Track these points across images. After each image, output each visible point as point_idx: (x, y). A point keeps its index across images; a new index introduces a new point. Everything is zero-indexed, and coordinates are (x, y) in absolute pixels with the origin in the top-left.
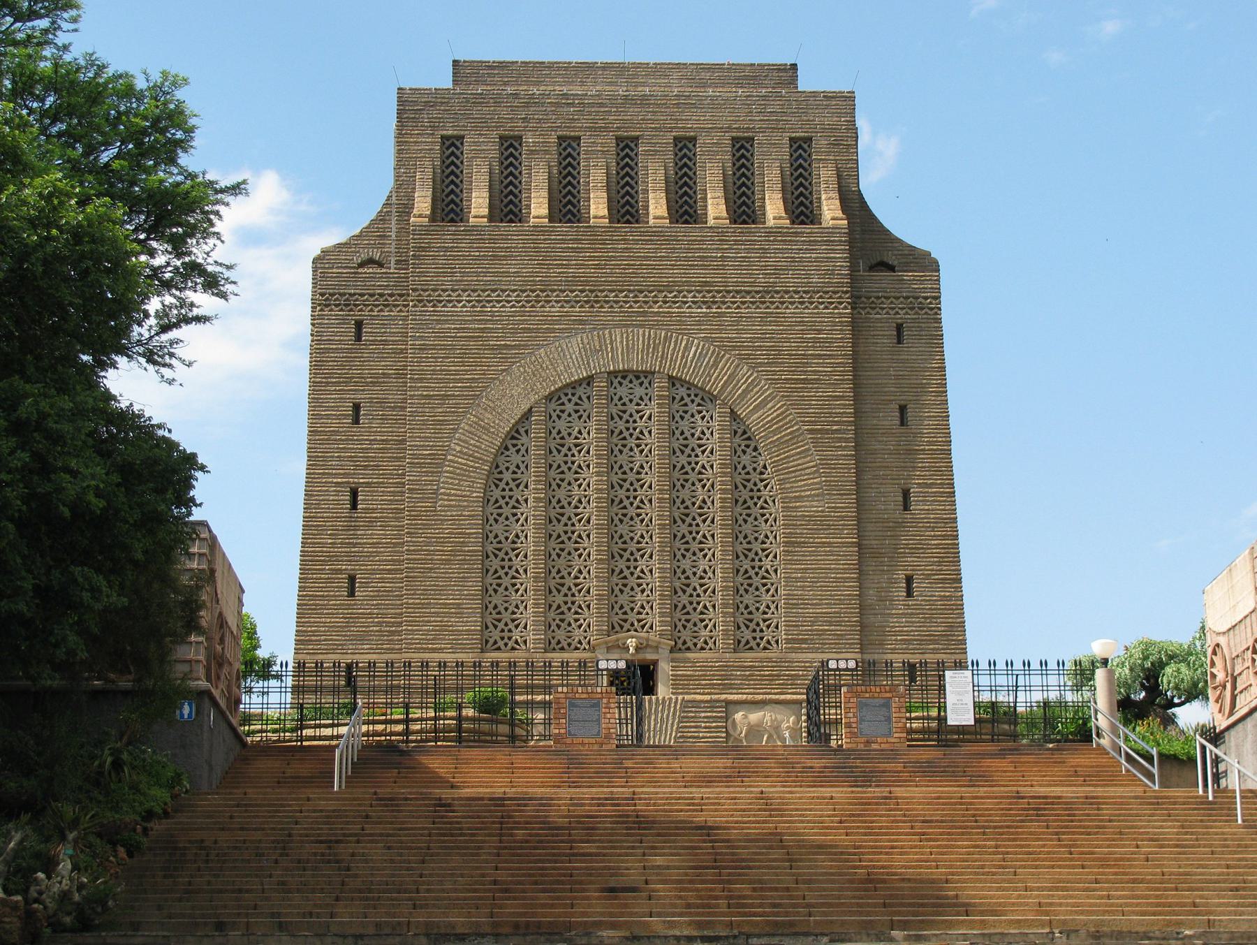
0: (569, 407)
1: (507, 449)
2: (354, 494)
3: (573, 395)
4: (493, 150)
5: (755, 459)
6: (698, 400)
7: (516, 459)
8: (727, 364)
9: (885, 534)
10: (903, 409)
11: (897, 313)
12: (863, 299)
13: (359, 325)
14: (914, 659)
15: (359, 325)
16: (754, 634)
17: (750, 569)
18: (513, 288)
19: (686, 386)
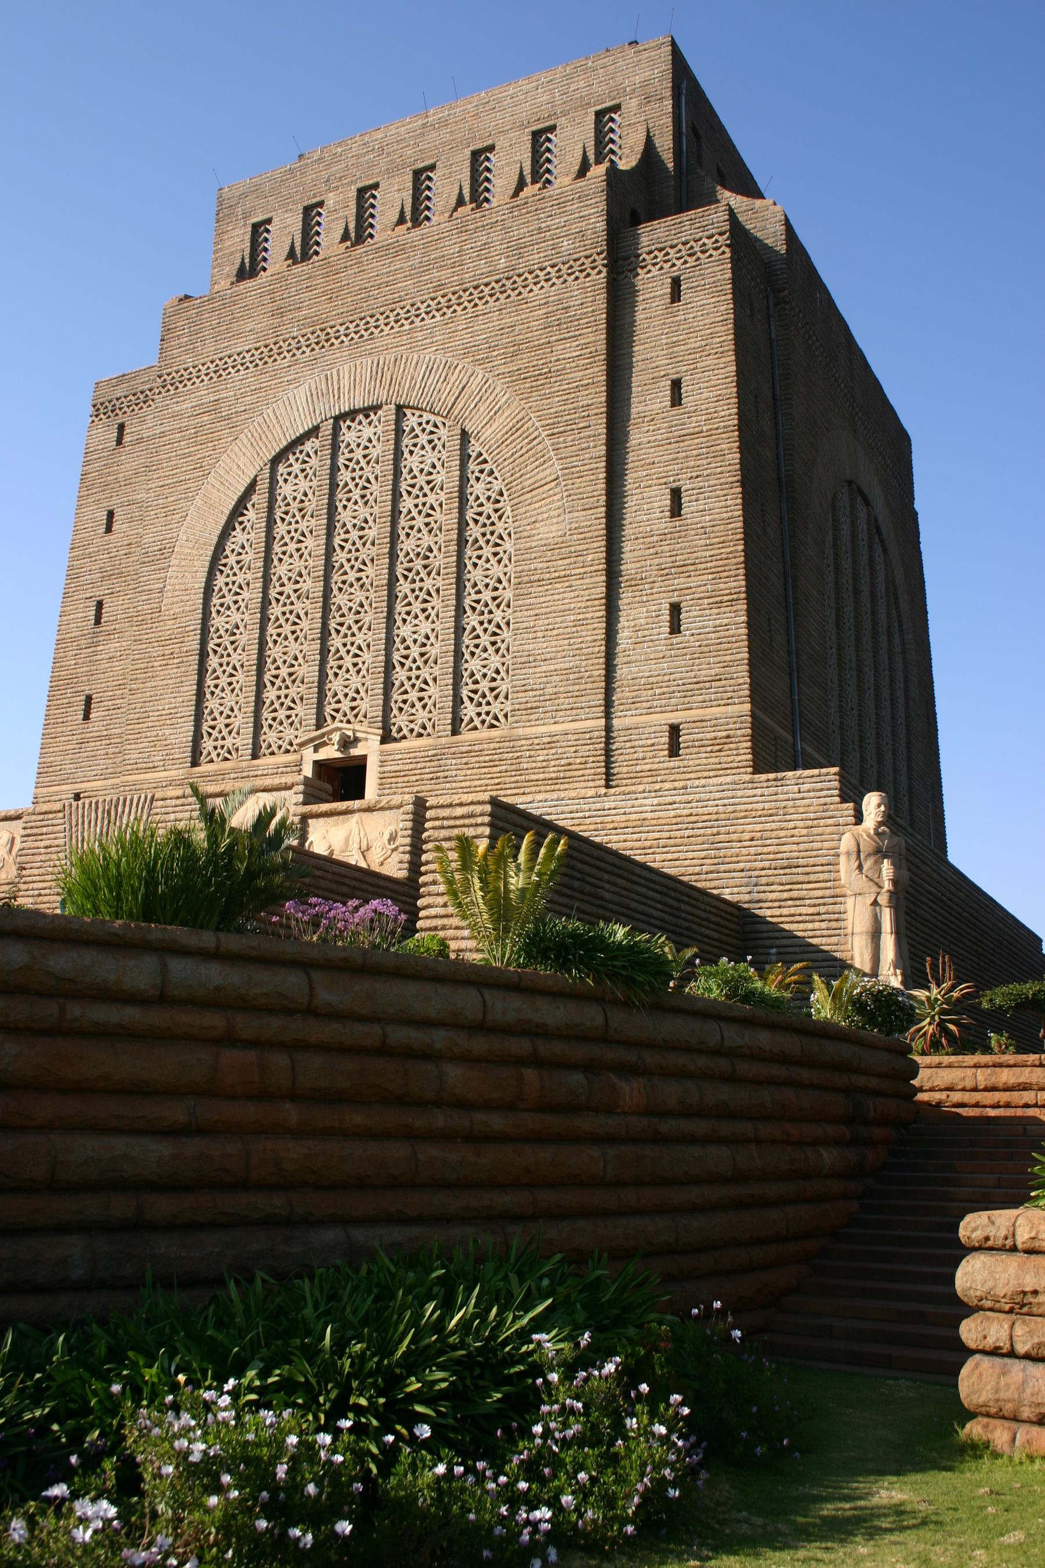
2: (100, 605)
3: (301, 452)
4: (295, 222)
5: (489, 486)
9: (648, 552)
10: (676, 385)
11: (674, 265)
12: (633, 259)
13: (121, 427)
14: (674, 718)
15: (121, 427)
16: (479, 709)
17: (477, 626)
18: (247, 348)
19: (417, 413)
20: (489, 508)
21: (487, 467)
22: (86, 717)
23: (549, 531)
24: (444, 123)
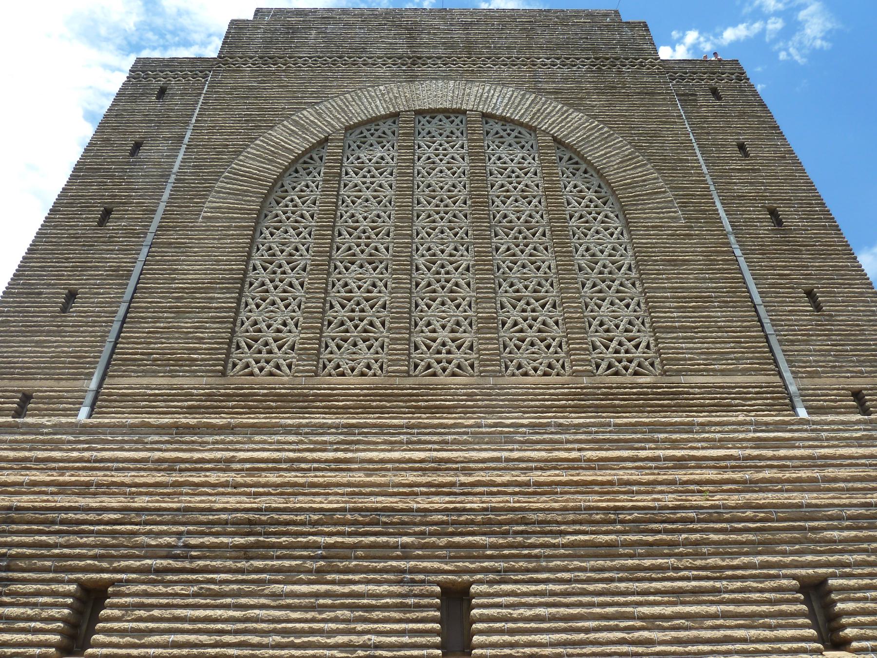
1: (297, 171)
6: (514, 134)
19: (500, 123)
21: (583, 167)
22: (65, 309)
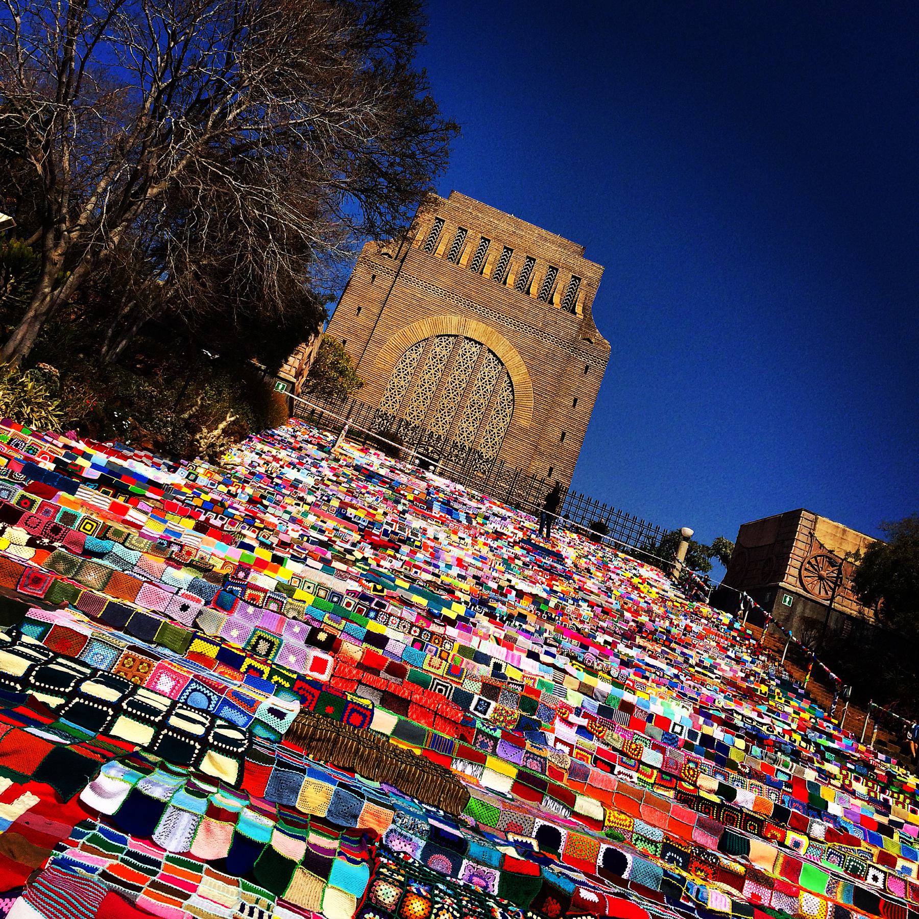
0: (444, 344)
1: (412, 350)
7: (414, 356)
8: (514, 353)
10: (575, 400)
13: (374, 277)
15: (374, 277)
20: (506, 402)
23: (524, 423)
24: (522, 237)
